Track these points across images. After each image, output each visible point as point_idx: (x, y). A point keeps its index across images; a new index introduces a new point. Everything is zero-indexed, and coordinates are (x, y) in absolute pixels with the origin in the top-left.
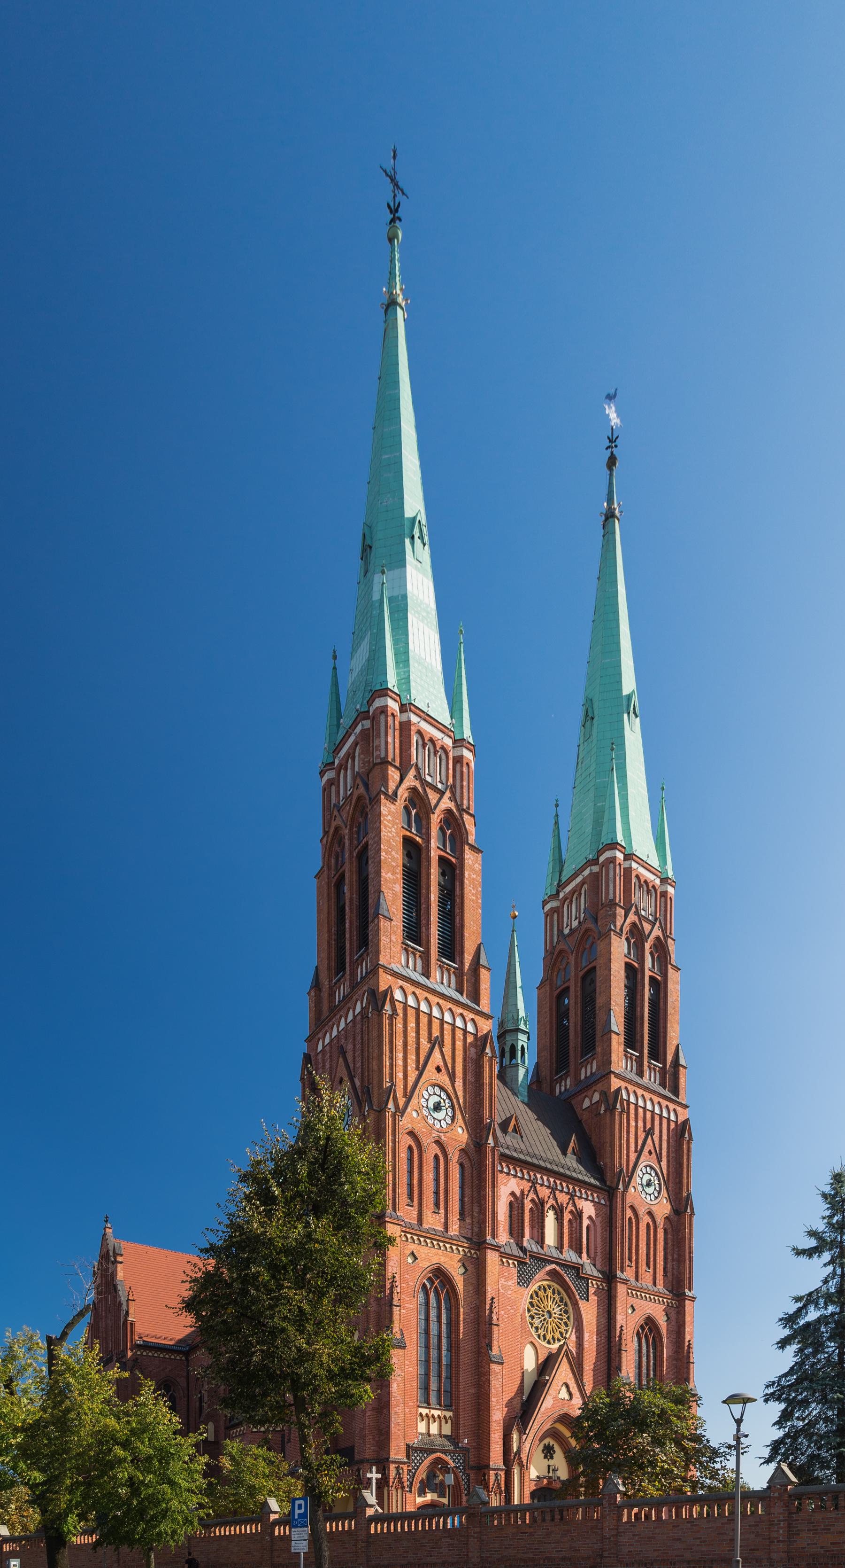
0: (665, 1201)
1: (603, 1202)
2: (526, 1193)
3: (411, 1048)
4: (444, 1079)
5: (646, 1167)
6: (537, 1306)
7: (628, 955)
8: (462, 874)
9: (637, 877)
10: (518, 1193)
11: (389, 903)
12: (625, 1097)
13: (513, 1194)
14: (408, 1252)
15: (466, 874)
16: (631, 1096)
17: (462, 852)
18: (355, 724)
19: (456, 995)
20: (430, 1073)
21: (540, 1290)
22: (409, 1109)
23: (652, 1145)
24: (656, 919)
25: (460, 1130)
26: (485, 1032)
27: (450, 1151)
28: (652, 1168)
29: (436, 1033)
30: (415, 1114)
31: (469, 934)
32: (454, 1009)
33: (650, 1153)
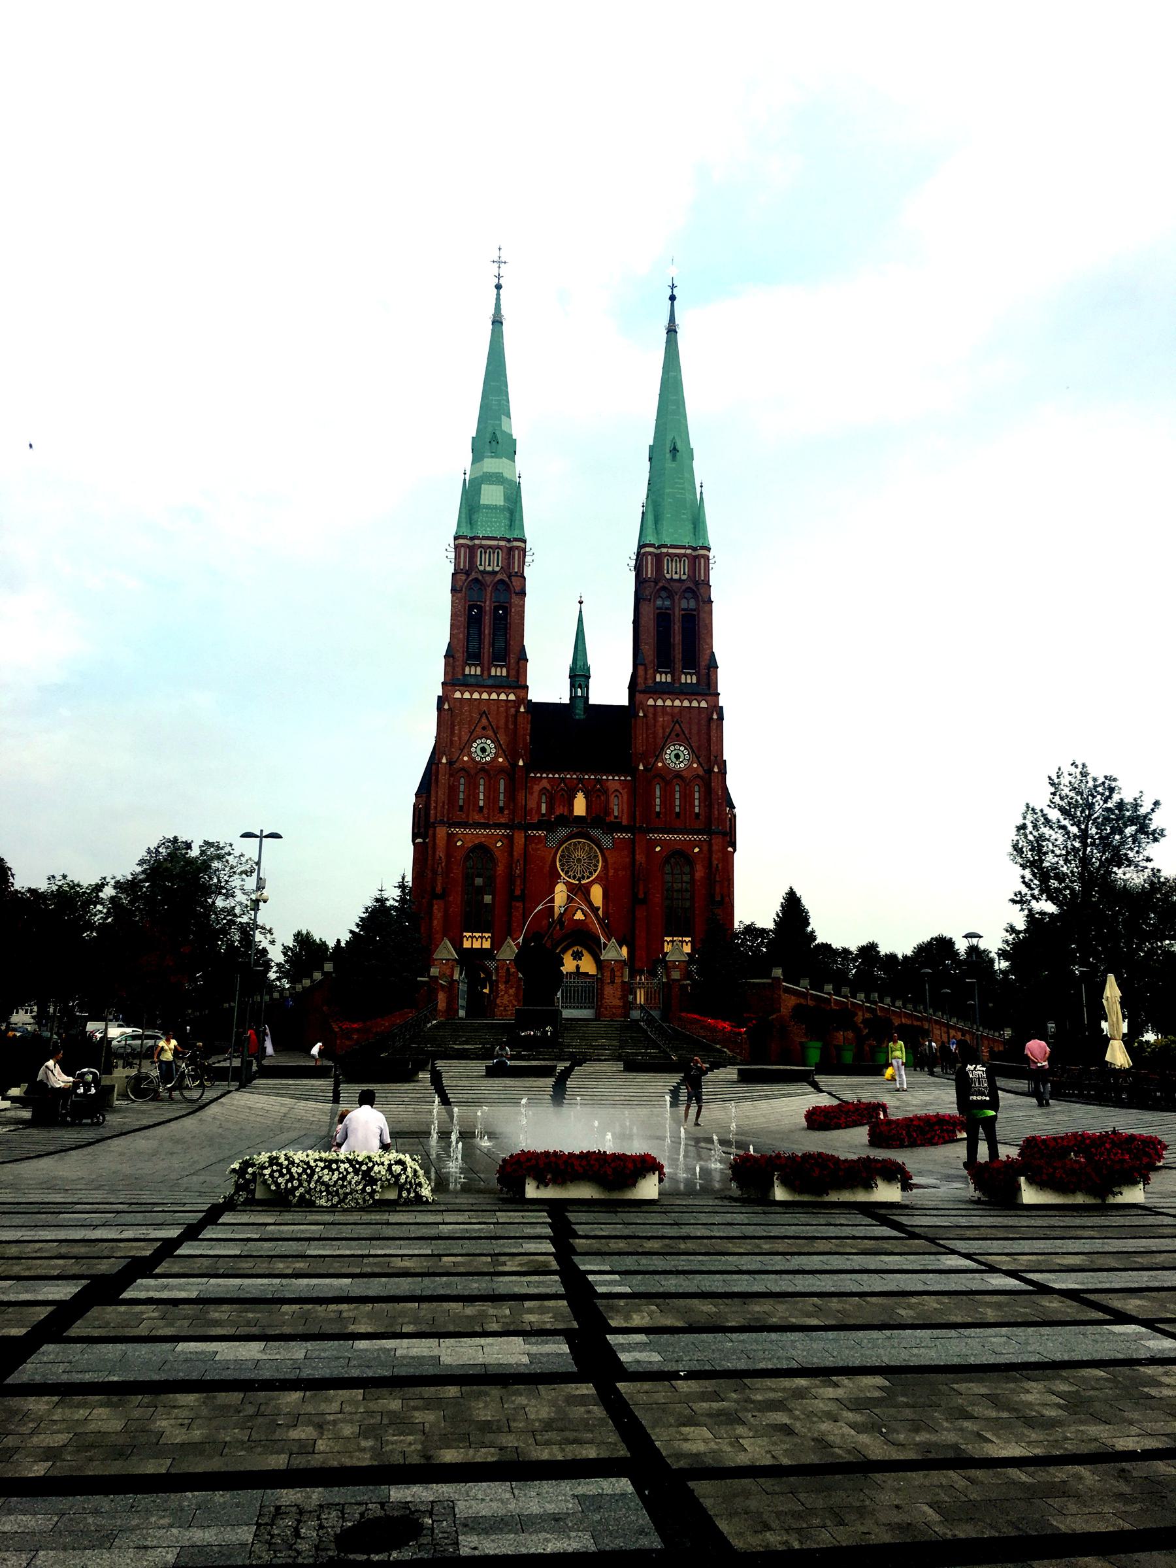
0: (695, 765)
4: (490, 733)
6: (568, 856)
8: (511, 610)
23: (679, 729)
33: (677, 735)
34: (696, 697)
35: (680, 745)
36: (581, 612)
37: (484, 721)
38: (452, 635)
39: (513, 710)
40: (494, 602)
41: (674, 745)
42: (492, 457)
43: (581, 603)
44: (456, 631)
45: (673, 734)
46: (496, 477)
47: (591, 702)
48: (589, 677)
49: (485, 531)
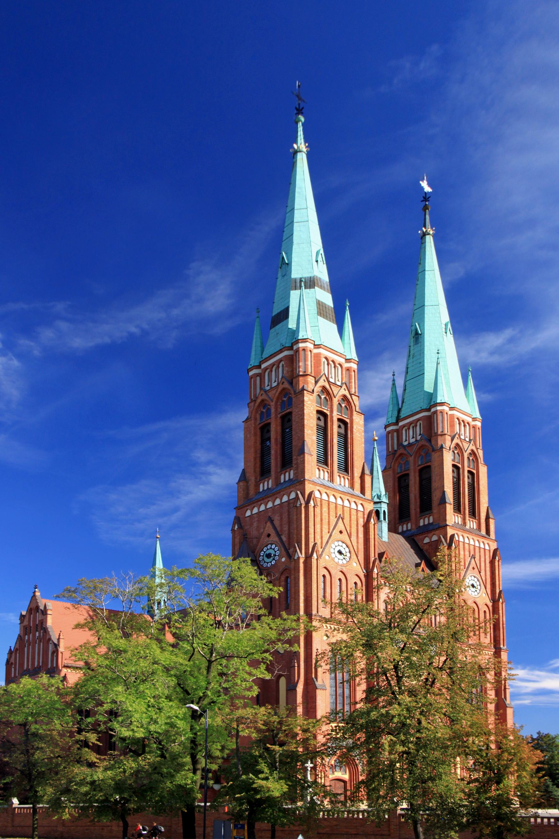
0: (484, 595)
3: (325, 521)
4: (345, 537)
5: (471, 576)
7: (454, 460)
9: (458, 419)
11: (309, 446)
12: (457, 539)
16: (460, 537)
18: (281, 351)
22: (324, 555)
24: (470, 440)
26: (369, 510)
29: (340, 512)
30: (327, 558)
32: (350, 499)
33: (473, 568)
37: (340, 526)
39: (361, 522)
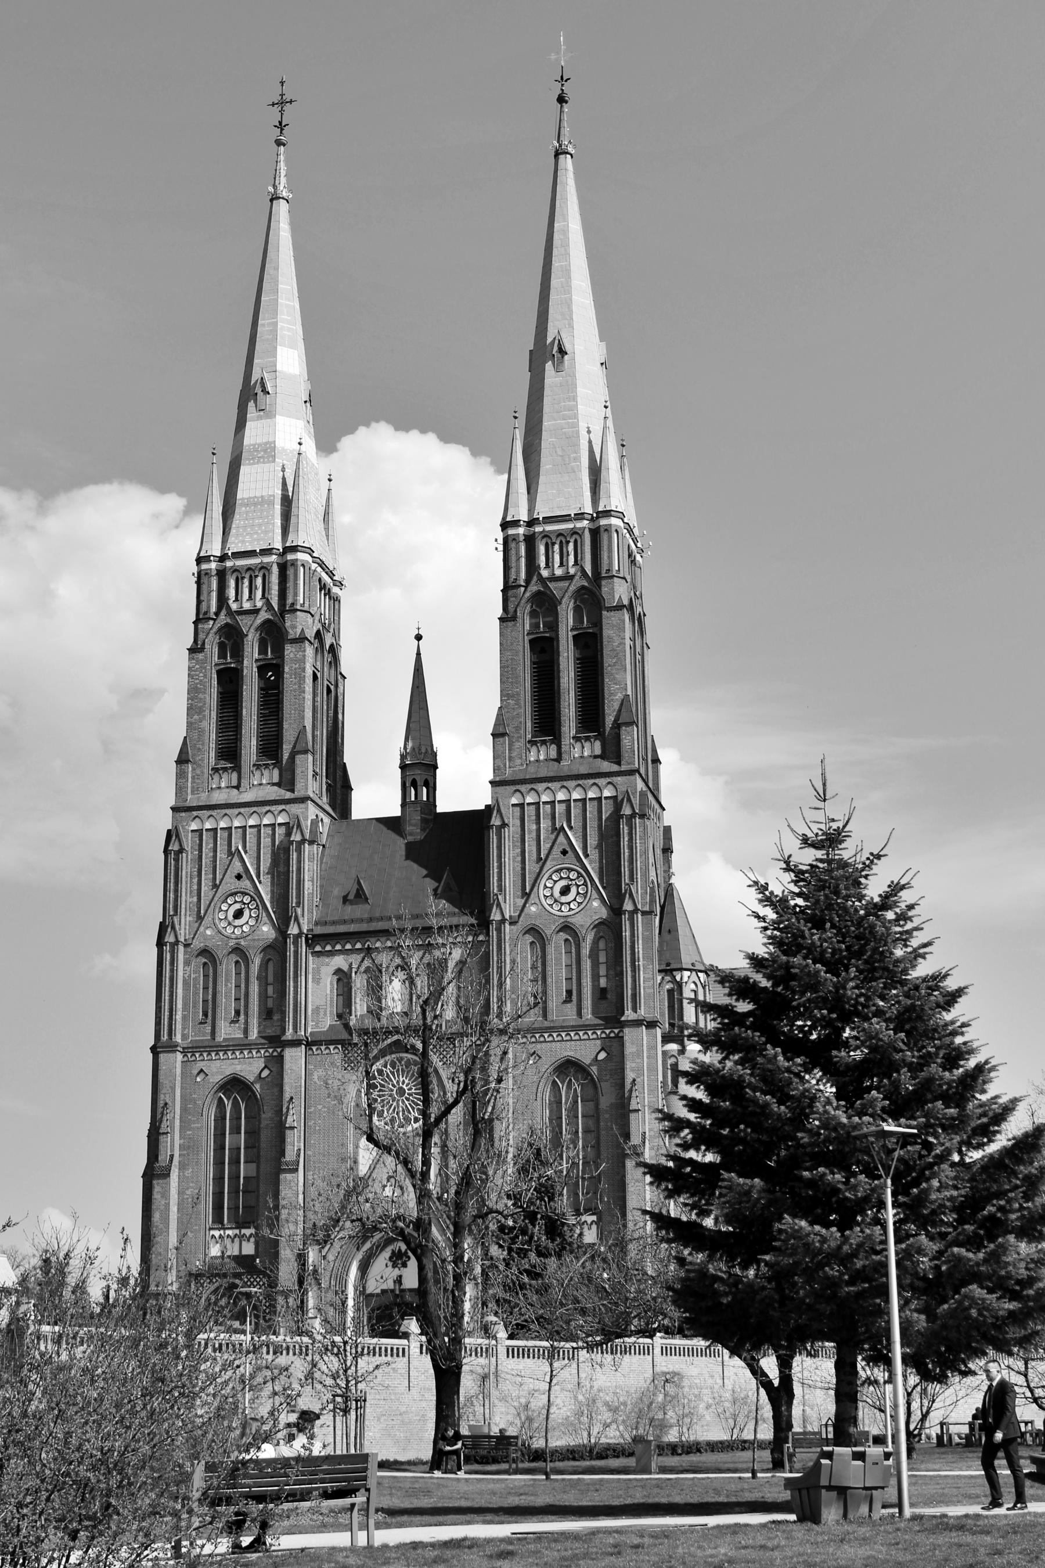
1: (481, 938)
2: (355, 966)
10: (345, 968)
13: (338, 971)
14: (195, 1072)
15: (287, 669)
17: (284, 649)
19: (275, 793)
20: (230, 884)
21: (386, 1067)
23: (565, 842)
25: (265, 929)
27: (251, 953)
28: (570, 870)
29: (237, 843)
31: (290, 724)
33: (564, 852)
34: (597, 781)
35: (570, 870)
36: (418, 654)
38: (190, 725)
40: (257, 660)
41: (559, 871)
42: (260, 418)
43: (419, 637)
44: (196, 717)
45: (557, 851)
46: (265, 451)
47: (439, 810)
48: (435, 767)
49: (243, 542)
